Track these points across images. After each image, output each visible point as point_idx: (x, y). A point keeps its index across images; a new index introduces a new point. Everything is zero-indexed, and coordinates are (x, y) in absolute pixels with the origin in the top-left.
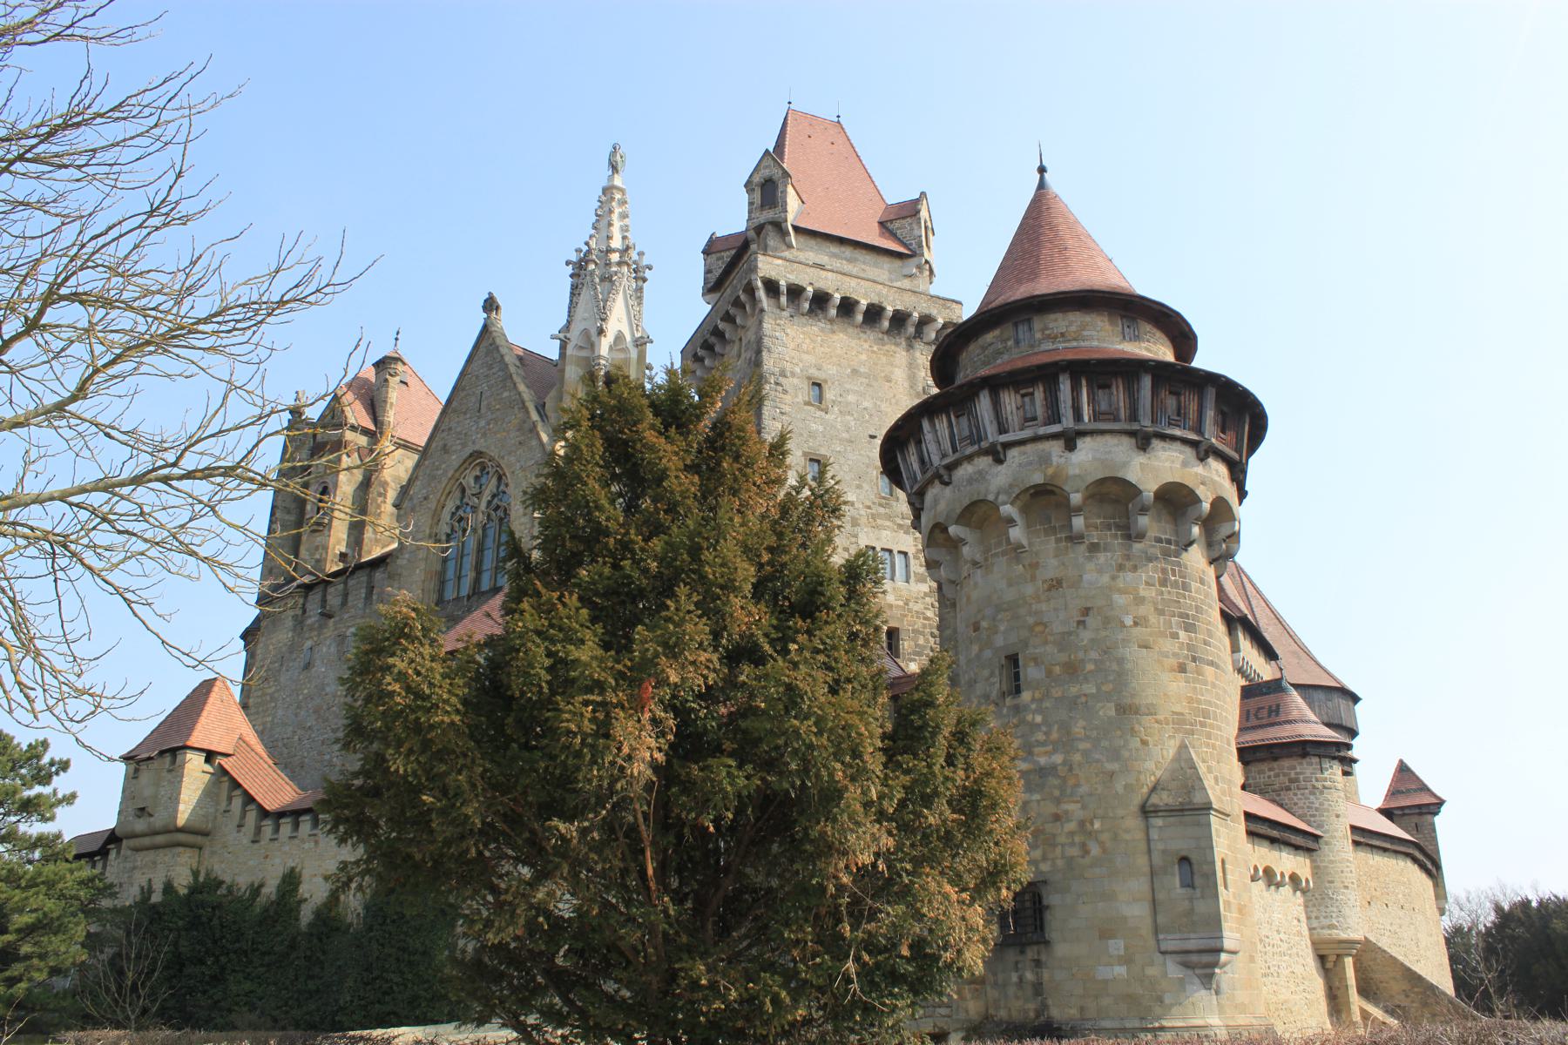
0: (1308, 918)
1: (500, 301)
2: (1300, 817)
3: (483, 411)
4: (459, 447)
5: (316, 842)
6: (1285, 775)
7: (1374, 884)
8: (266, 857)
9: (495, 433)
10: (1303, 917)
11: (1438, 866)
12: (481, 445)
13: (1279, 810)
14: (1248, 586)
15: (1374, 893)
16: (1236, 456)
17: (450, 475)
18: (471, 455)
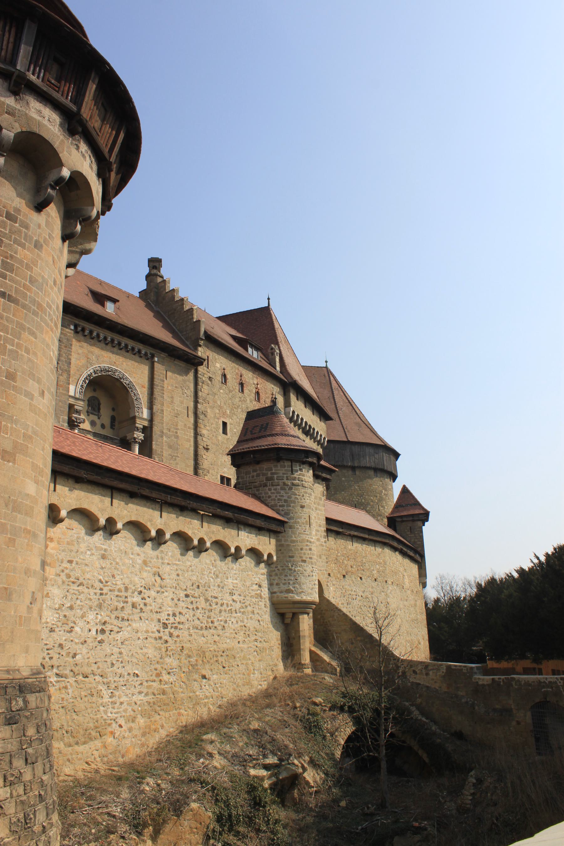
0: (271, 584)
2: (272, 507)
6: (264, 475)
7: (350, 563)
10: (265, 584)
11: (422, 556)
13: (257, 503)
14: (333, 382)
15: (350, 569)
16: (74, 108)
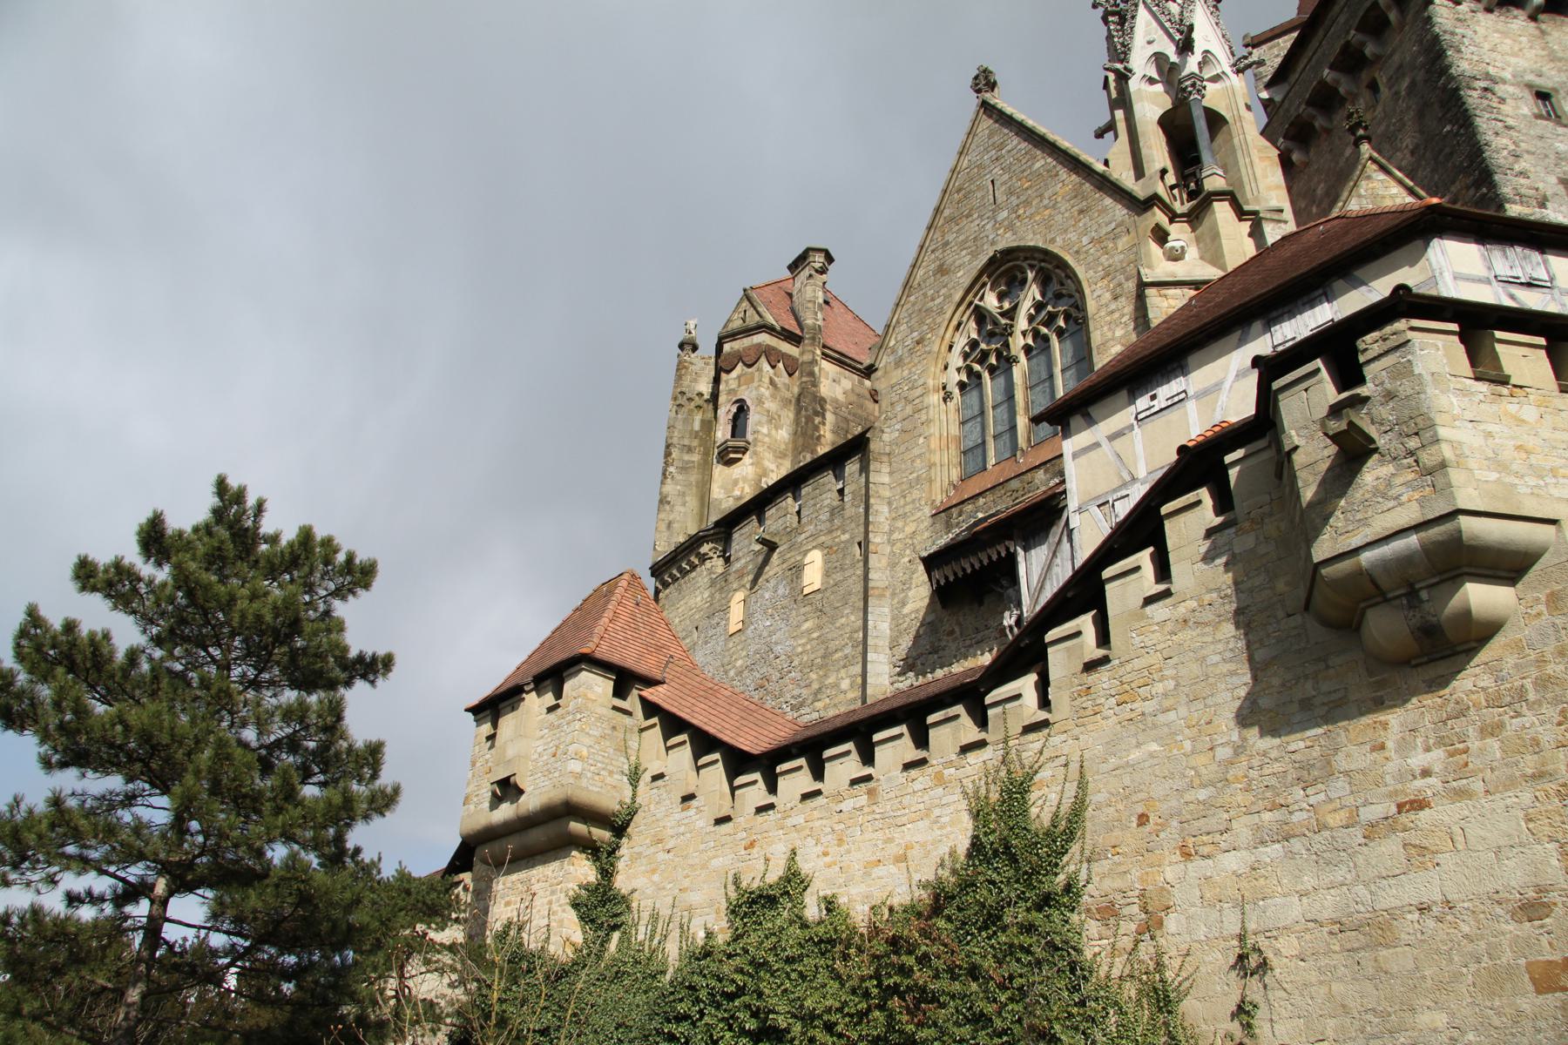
1: (998, 78)
3: (1001, 198)
4: (969, 257)
5: (871, 793)
8: (752, 845)
9: (1031, 217)
12: (1006, 241)
17: (958, 296)
18: (992, 261)
